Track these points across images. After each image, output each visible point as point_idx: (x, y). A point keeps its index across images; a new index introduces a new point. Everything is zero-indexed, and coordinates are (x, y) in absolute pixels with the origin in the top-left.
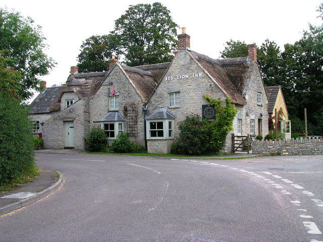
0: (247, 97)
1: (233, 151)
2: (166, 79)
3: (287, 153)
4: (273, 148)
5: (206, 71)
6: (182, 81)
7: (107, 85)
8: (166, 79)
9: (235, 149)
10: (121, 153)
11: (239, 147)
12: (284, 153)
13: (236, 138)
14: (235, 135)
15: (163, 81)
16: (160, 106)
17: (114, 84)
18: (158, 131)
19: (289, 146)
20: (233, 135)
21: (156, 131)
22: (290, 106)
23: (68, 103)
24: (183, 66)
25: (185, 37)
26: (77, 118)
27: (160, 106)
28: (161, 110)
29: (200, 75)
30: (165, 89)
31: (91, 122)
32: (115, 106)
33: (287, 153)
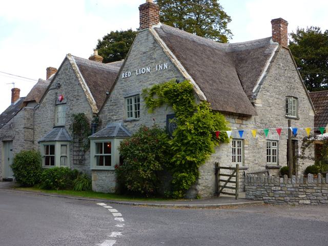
0: (259, 103)
1: (217, 192)
2: (123, 76)
3: (308, 202)
4: (281, 190)
5: (268, 64)
6: (141, 77)
7: (56, 88)
8: (123, 76)
9: (221, 188)
10: (48, 188)
11: (229, 181)
12: (301, 202)
13: (222, 171)
14: (221, 166)
15: (120, 78)
16: (115, 118)
17: (63, 86)
18: (106, 156)
19: (312, 187)
20: (217, 165)
21: (103, 156)
22: (93, 131)
23: (139, 114)
24: (145, 53)
25: (149, 7)
26: (17, 137)
27: (115, 118)
28: (115, 124)
29: (166, 66)
30: (121, 93)
31: (36, 142)
32: (134, 114)
33: (308, 202)
